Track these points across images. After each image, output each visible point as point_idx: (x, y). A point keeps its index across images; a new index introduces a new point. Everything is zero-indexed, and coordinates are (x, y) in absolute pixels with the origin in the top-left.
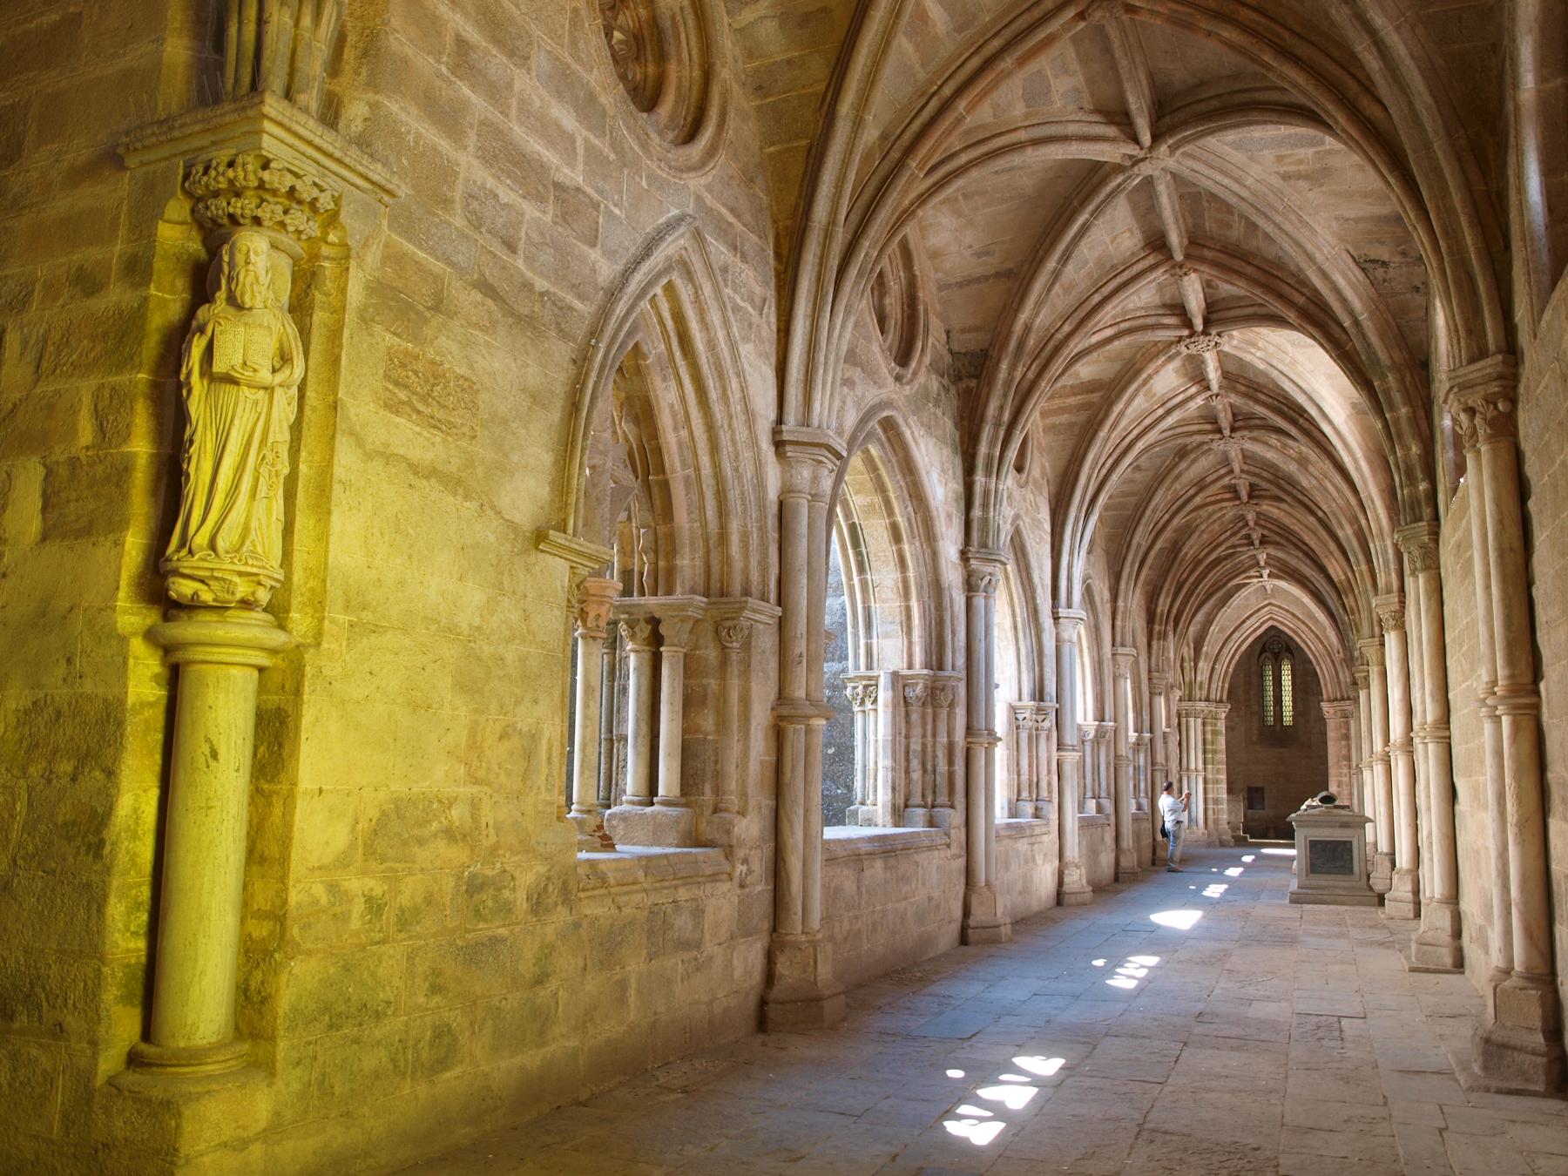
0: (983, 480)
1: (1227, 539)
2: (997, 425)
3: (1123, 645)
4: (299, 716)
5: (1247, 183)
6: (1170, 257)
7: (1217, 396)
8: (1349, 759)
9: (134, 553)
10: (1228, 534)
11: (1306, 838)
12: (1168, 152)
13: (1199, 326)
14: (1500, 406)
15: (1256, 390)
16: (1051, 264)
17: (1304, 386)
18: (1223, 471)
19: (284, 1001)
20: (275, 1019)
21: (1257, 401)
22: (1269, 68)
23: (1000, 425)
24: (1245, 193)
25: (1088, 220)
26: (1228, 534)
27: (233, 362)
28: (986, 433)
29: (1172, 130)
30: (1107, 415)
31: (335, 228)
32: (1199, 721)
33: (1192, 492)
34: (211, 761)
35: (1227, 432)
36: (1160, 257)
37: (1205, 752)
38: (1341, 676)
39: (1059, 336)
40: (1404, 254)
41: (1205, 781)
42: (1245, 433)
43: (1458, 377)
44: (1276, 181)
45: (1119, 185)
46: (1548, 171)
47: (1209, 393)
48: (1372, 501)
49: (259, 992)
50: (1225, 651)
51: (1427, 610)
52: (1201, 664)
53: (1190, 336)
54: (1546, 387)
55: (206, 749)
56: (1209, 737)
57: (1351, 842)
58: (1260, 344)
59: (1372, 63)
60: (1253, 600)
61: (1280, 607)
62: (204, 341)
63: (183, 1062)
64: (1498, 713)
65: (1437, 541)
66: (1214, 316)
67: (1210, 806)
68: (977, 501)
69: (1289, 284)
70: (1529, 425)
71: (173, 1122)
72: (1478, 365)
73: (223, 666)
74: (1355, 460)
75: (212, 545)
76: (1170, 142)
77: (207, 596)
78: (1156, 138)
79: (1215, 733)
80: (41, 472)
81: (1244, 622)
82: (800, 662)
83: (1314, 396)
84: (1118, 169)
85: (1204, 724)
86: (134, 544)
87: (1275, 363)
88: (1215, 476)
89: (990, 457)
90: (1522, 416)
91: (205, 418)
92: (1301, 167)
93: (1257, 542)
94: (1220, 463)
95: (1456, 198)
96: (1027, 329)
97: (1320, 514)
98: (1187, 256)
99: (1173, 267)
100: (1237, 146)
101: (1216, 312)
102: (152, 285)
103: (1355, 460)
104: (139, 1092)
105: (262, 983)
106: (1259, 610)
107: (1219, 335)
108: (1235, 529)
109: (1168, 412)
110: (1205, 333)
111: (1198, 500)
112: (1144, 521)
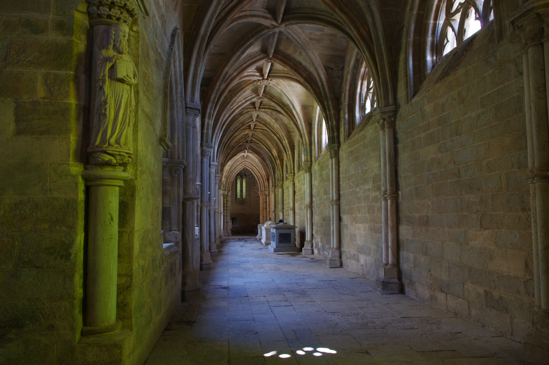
0: (207, 120)
1: (243, 140)
2: (213, 103)
3: (217, 173)
4: (134, 204)
5: (301, 39)
6: (268, 56)
7: (261, 98)
8: (266, 209)
9: (73, 143)
10: (243, 139)
11: (278, 232)
12: (284, 26)
13: (266, 77)
14: (392, 119)
15: (272, 97)
16: (238, 54)
17: (290, 98)
18: (250, 120)
19: (133, 305)
20: (131, 311)
21: (273, 101)
22: (335, 12)
23: (214, 103)
24: (300, 42)
25: (253, 41)
26: (243, 139)
27: (124, 75)
28: (210, 105)
29: (288, 20)
30: (230, 101)
31: (135, 25)
33: (240, 126)
34: (111, 221)
35: (257, 109)
36: (265, 55)
38: (265, 184)
39: (233, 76)
40: (337, 67)
41: (224, 216)
42: (263, 110)
43: (382, 110)
44: (307, 39)
45: (266, 33)
46: (413, 61)
47: (259, 97)
48: (305, 135)
49: (122, 303)
51: (335, 169)
53: (262, 80)
54: (413, 117)
55: (109, 217)
56: (225, 202)
57: (290, 234)
58: (280, 85)
59: (369, 19)
60: (240, 159)
62: (111, 64)
63: (110, 330)
64: (387, 199)
65: (339, 149)
66: (271, 75)
67: (225, 224)
68: (206, 128)
69: (302, 70)
70: (400, 125)
71: (118, 351)
72: (386, 108)
73: (114, 187)
74: (301, 122)
75: (118, 142)
76: (287, 23)
77: (114, 161)
78: (283, 21)
79: (227, 201)
80: (13, 105)
82: (191, 181)
83: (293, 102)
84: (267, 28)
86: (73, 139)
87: (283, 91)
88: (248, 121)
89: (210, 113)
90: (397, 123)
91: (110, 94)
92: (316, 37)
93: (249, 142)
94: (249, 117)
95: (386, 61)
96: (227, 73)
97: (278, 135)
98: (273, 56)
99: (269, 59)
100: (300, 28)
101: (271, 73)
102: (74, 36)
103: (301, 122)
104: (99, 343)
105: (124, 299)
106: (242, 163)
107: (271, 80)
108: (245, 138)
109: (246, 102)
110: (267, 79)
111: (242, 128)
112: (227, 134)
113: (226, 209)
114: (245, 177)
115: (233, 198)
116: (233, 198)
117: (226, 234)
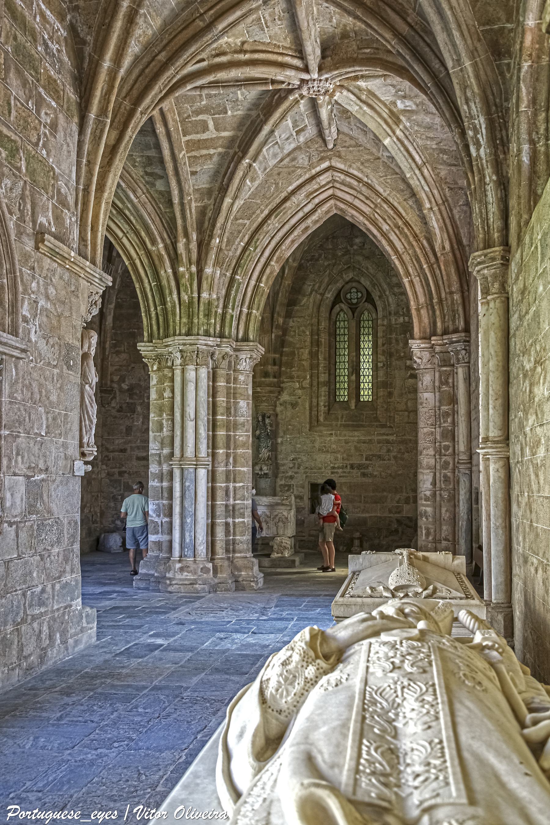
32: (204, 372)
37: (213, 425)
41: (212, 477)
50: (254, 252)
52: (208, 270)
56: (221, 399)
61: (348, 174)
81: (286, 199)
85: (214, 377)
113: (228, 437)
114: (370, 306)
115: (314, 400)
116: (314, 400)
117: (223, 575)
